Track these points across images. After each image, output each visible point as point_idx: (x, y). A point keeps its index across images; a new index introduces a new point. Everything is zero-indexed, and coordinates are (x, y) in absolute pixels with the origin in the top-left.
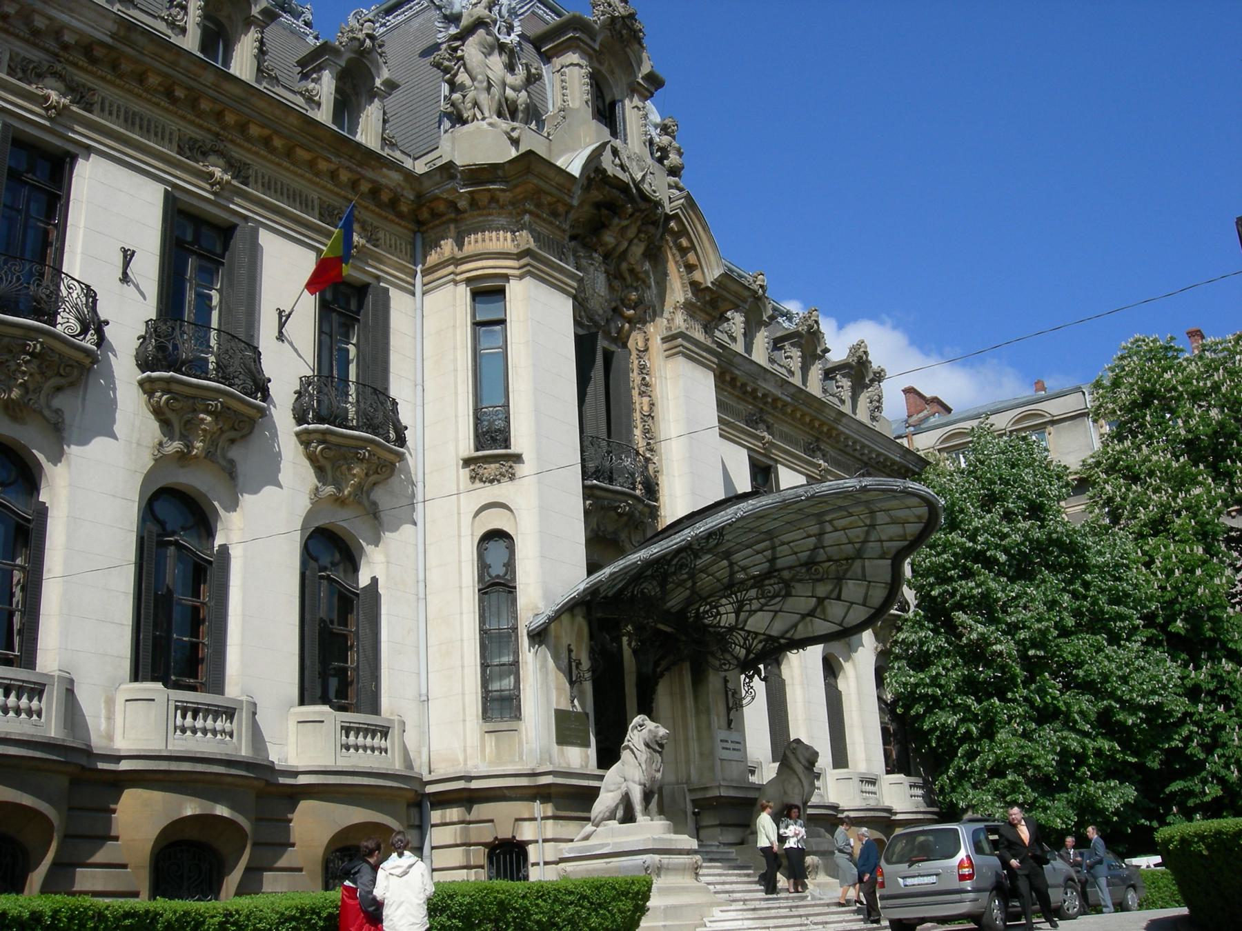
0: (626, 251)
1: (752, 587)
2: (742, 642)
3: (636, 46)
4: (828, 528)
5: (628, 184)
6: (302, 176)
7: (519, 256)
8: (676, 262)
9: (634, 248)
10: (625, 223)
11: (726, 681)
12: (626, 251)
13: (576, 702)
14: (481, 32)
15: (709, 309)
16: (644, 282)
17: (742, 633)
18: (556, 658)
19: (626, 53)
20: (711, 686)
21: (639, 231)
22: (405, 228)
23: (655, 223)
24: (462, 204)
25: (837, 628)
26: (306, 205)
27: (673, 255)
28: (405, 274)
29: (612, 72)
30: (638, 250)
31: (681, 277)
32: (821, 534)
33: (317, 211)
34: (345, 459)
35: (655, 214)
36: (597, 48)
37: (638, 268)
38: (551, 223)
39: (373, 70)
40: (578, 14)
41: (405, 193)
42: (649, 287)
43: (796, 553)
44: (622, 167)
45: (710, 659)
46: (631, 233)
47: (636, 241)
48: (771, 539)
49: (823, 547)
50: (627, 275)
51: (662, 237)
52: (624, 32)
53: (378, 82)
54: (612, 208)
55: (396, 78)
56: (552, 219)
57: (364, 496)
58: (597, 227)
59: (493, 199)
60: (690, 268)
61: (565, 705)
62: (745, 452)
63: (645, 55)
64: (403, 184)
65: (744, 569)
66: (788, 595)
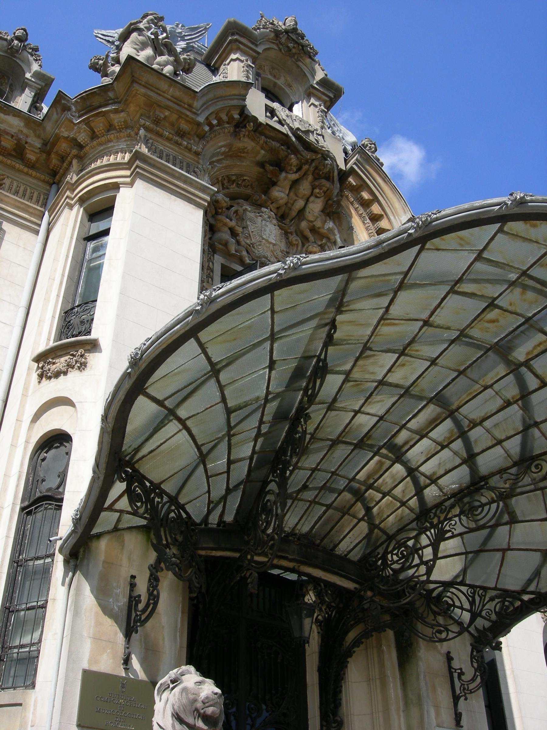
0: (301, 212)
1: (452, 506)
2: (467, 605)
3: (308, 61)
4: (532, 383)
5: (287, 135)
7: (128, 165)
8: (360, 216)
9: (311, 206)
10: (294, 176)
11: (449, 658)
12: (301, 212)
13: (135, 663)
14: (135, 35)
16: (328, 239)
17: (464, 589)
18: (102, 593)
19: (298, 67)
20: (422, 666)
22: (38, 179)
24: (82, 138)
27: (356, 209)
28: (31, 214)
29: (290, 86)
30: (316, 207)
31: (367, 229)
32: (525, 395)
35: (325, 166)
36: (260, 50)
37: (318, 224)
38: (177, 143)
39: (24, 67)
40: (232, 19)
41: (29, 140)
43: (499, 442)
44: (280, 122)
45: (420, 627)
46: (305, 188)
47: (312, 199)
48: (451, 414)
49: (536, 424)
51: (341, 193)
52: (291, 45)
53: (28, 75)
55: (48, 72)
56: (176, 138)
58: (268, 185)
59: (110, 127)
60: (375, 219)
61: (109, 664)
63: (317, 66)
64: (25, 131)
65: (434, 480)
66: (514, 520)
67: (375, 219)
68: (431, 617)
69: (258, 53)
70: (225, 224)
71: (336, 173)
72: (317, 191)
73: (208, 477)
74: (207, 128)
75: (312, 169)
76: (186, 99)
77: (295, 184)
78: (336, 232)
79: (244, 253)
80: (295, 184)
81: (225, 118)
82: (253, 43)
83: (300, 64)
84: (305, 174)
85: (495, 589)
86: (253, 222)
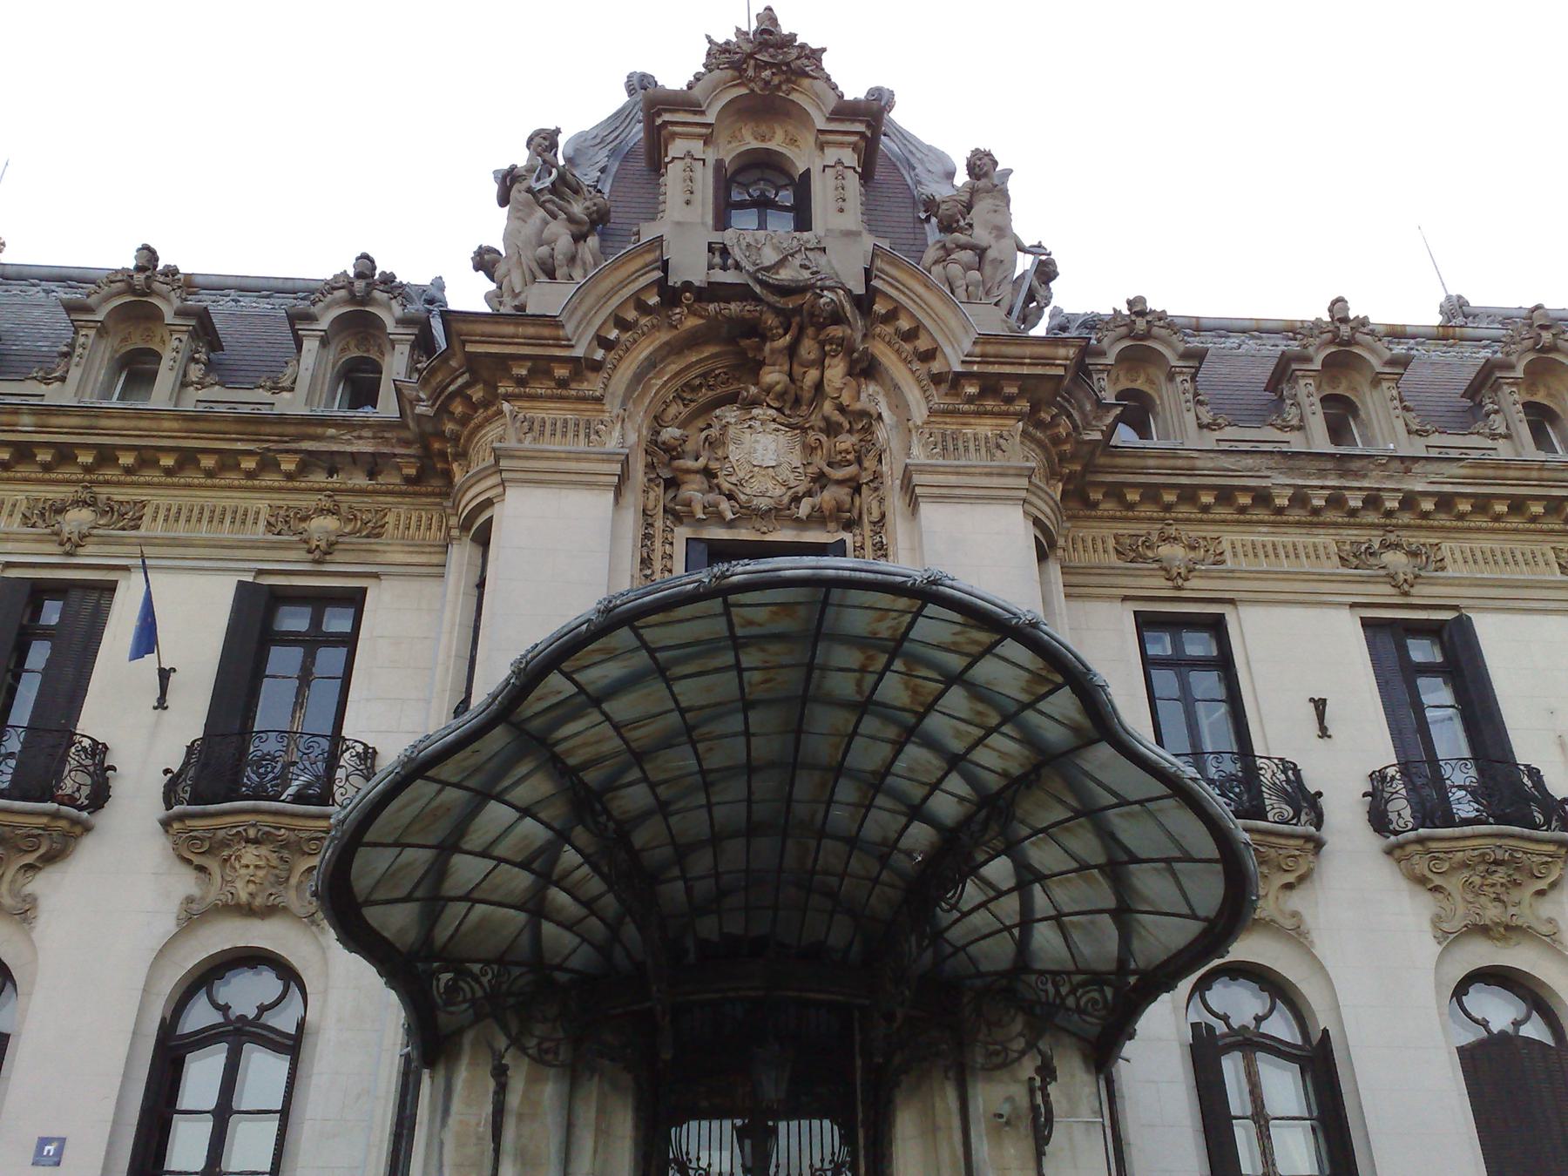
3: (806, 82)
6: (230, 487)
9: (828, 373)
12: (819, 386)
15: (990, 404)
16: (871, 416)
21: (822, 344)
23: (837, 318)
25: (1195, 928)
26: (241, 518)
30: (836, 372)
33: (262, 524)
34: (229, 846)
36: (710, 118)
37: (846, 399)
38: (562, 398)
42: (880, 416)
46: (808, 349)
50: (837, 417)
54: (754, 329)
57: (292, 894)
60: (928, 356)
62: (1345, 613)
67: (928, 356)
68: (984, 1029)
69: (710, 125)
70: (688, 471)
71: (848, 307)
72: (827, 348)
73: (568, 927)
74: (599, 354)
75: (806, 320)
76: (546, 332)
77: (792, 351)
78: (881, 399)
79: (725, 506)
80: (792, 351)
81: (631, 315)
82: (695, 113)
83: (794, 96)
84: (801, 330)
85: (1079, 971)
86: (738, 442)
